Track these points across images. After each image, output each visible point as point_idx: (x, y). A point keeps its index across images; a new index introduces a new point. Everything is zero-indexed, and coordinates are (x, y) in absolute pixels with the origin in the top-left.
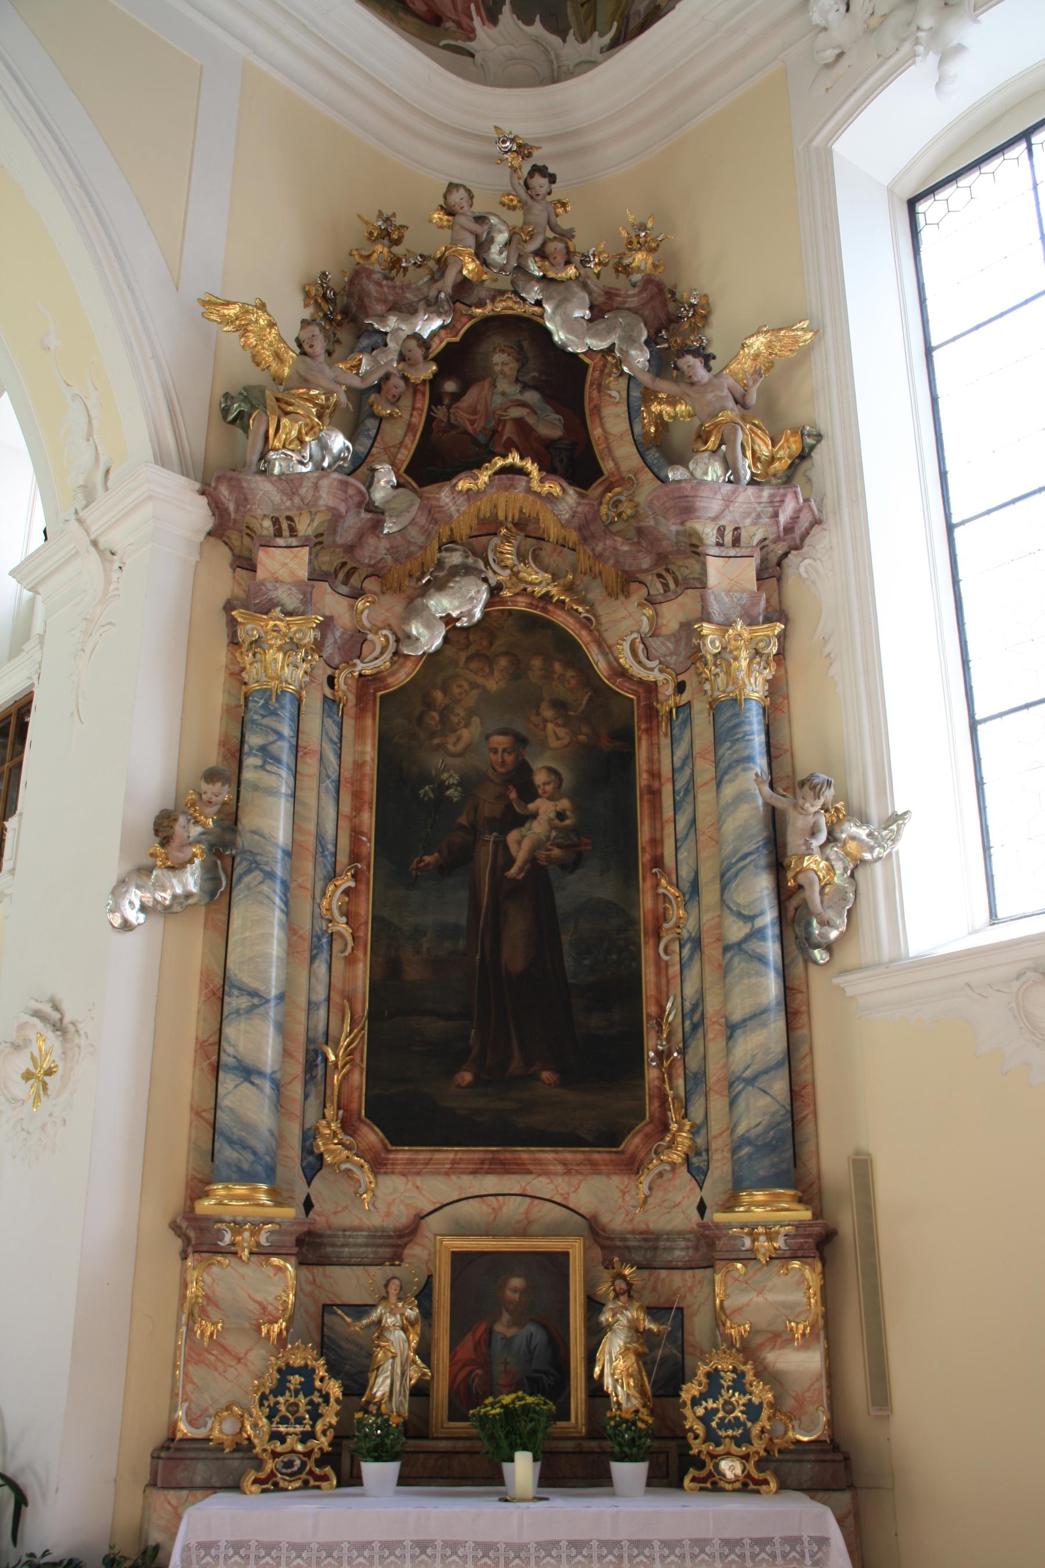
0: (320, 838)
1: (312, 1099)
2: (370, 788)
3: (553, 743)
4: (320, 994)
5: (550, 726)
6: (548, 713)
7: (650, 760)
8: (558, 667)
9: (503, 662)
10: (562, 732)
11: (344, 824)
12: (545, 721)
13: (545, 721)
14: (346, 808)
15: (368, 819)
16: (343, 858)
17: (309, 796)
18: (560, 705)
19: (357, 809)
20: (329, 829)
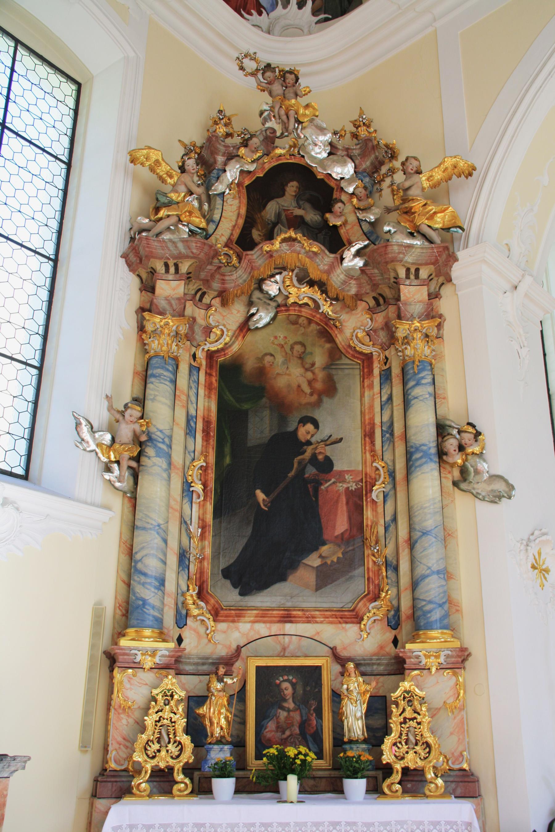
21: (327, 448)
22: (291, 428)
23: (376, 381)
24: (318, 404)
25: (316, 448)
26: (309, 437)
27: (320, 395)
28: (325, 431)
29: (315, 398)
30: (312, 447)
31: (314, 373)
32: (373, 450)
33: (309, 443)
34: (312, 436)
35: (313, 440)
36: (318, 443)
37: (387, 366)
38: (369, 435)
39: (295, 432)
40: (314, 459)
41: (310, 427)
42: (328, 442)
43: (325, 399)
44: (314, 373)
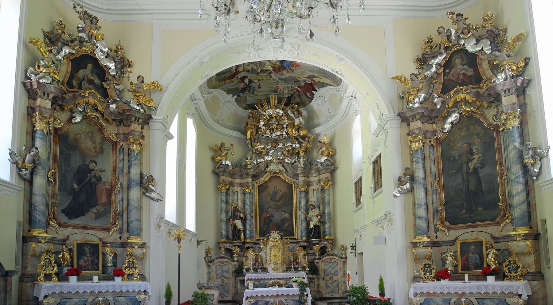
0: (431, 172)
1: (435, 219)
2: (440, 161)
3: (477, 143)
4: (435, 200)
5: (476, 139)
6: (475, 137)
7: (498, 142)
8: (476, 127)
9: (465, 128)
10: (478, 140)
11: (436, 168)
12: (475, 139)
13: (475, 139)
14: (436, 165)
15: (441, 167)
16: (437, 175)
17: (428, 165)
18: (478, 135)
19: (438, 165)
20: (433, 170)
21: (100, 173)
22: (87, 163)
23: (118, 152)
24: (97, 156)
25: (96, 172)
26: (93, 168)
27: (98, 153)
28: (99, 167)
29: (95, 154)
30: (94, 171)
31: (96, 145)
32: (115, 176)
33: (93, 170)
34: (95, 168)
35: (95, 169)
36: (97, 170)
37: (122, 148)
38: (115, 171)
39: (88, 165)
40: (95, 176)
41: (94, 164)
42: (100, 171)
43: (100, 155)
44: (96, 145)
